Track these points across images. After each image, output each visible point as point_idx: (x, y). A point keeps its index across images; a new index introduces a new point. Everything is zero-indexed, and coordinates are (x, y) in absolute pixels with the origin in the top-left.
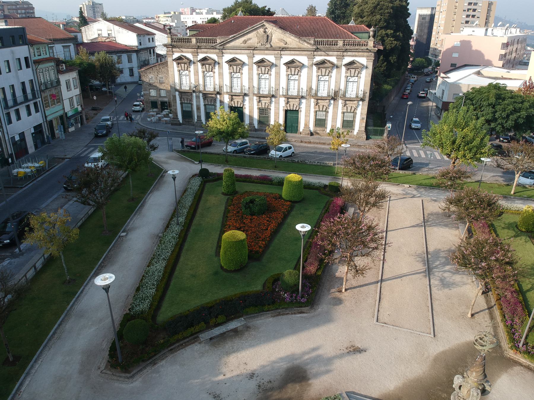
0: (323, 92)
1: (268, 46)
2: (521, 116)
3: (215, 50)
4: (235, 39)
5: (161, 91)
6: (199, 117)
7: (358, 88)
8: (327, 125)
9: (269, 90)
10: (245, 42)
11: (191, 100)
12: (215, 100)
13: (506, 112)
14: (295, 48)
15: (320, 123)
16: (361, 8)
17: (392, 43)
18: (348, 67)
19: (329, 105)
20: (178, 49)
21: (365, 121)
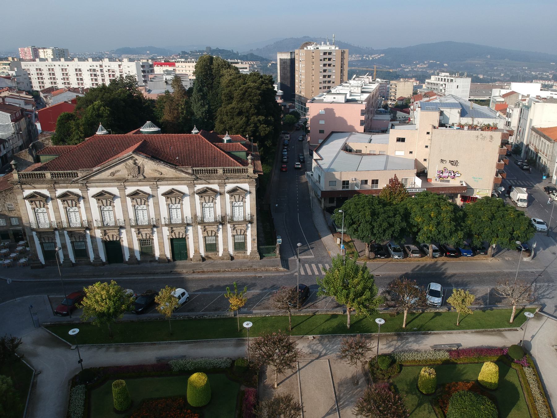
0: (210, 217)
2: (396, 230)
3: (77, 185)
4: (99, 172)
5: (11, 219)
6: (66, 256)
7: (244, 211)
8: (218, 249)
9: (149, 220)
10: (113, 174)
11: (54, 239)
12: (84, 236)
13: (383, 228)
14: (172, 178)
15: (211, 247)
16: (229, 89)
17: (266, 130)
18: (232, 194)
19: (218, 230)
20: (28, 186)
21: (256, 241)
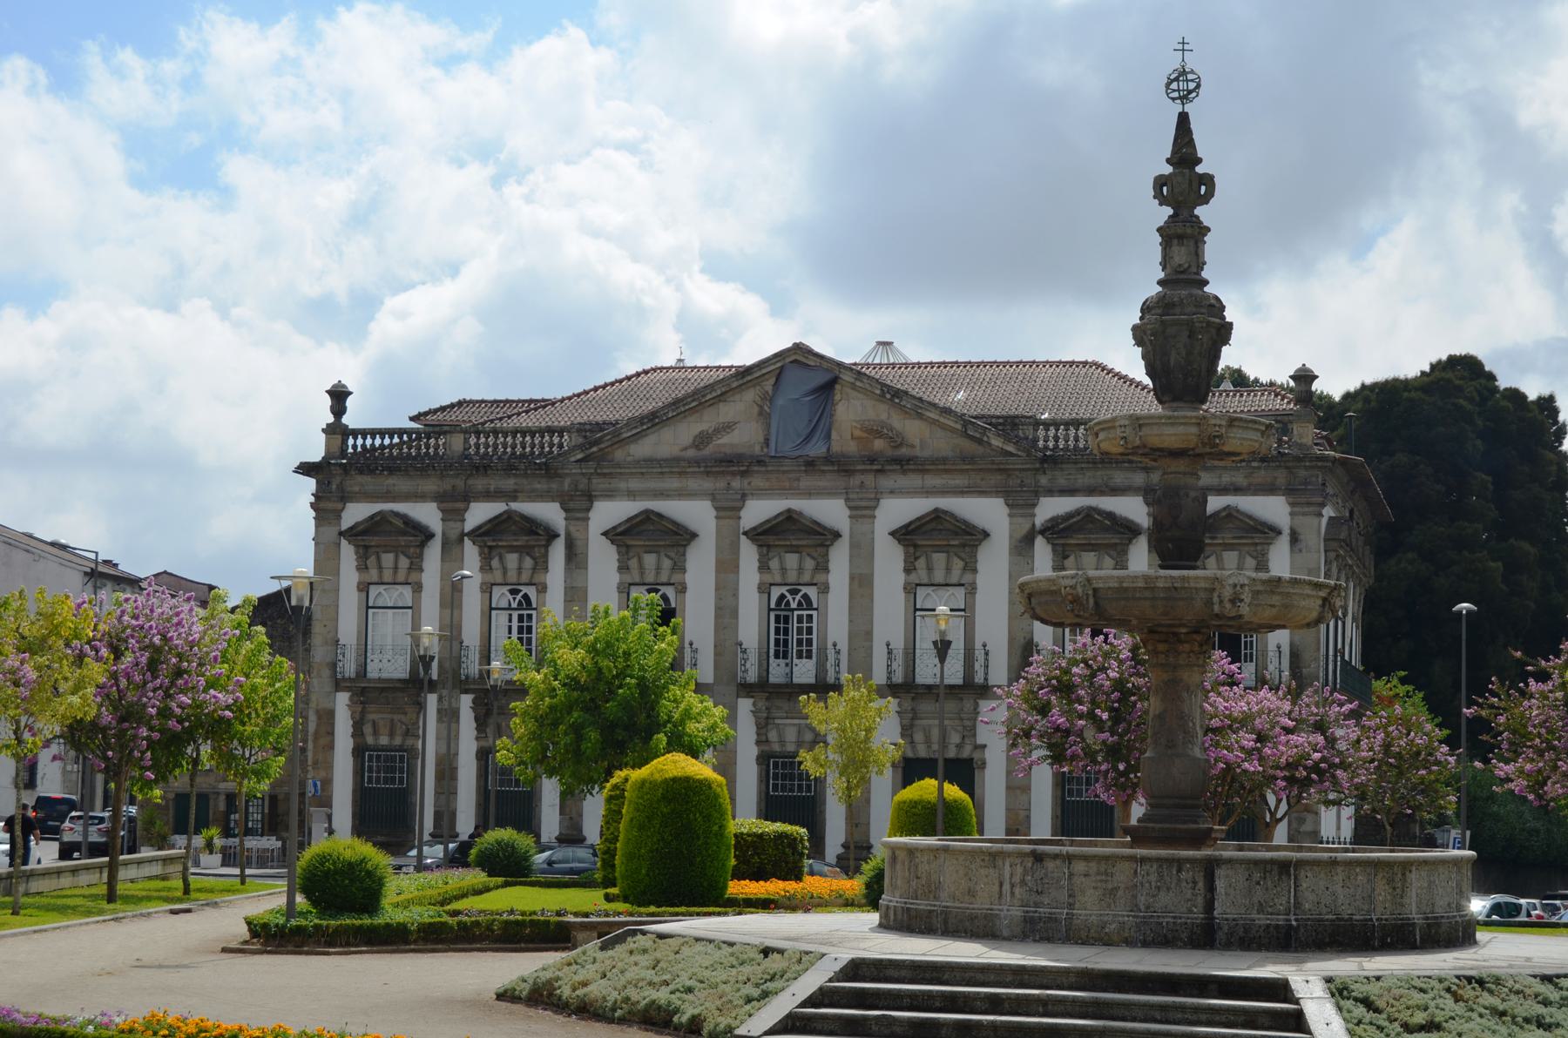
1: (816, 449)
10: (702, 440)
11: (412, 731)
